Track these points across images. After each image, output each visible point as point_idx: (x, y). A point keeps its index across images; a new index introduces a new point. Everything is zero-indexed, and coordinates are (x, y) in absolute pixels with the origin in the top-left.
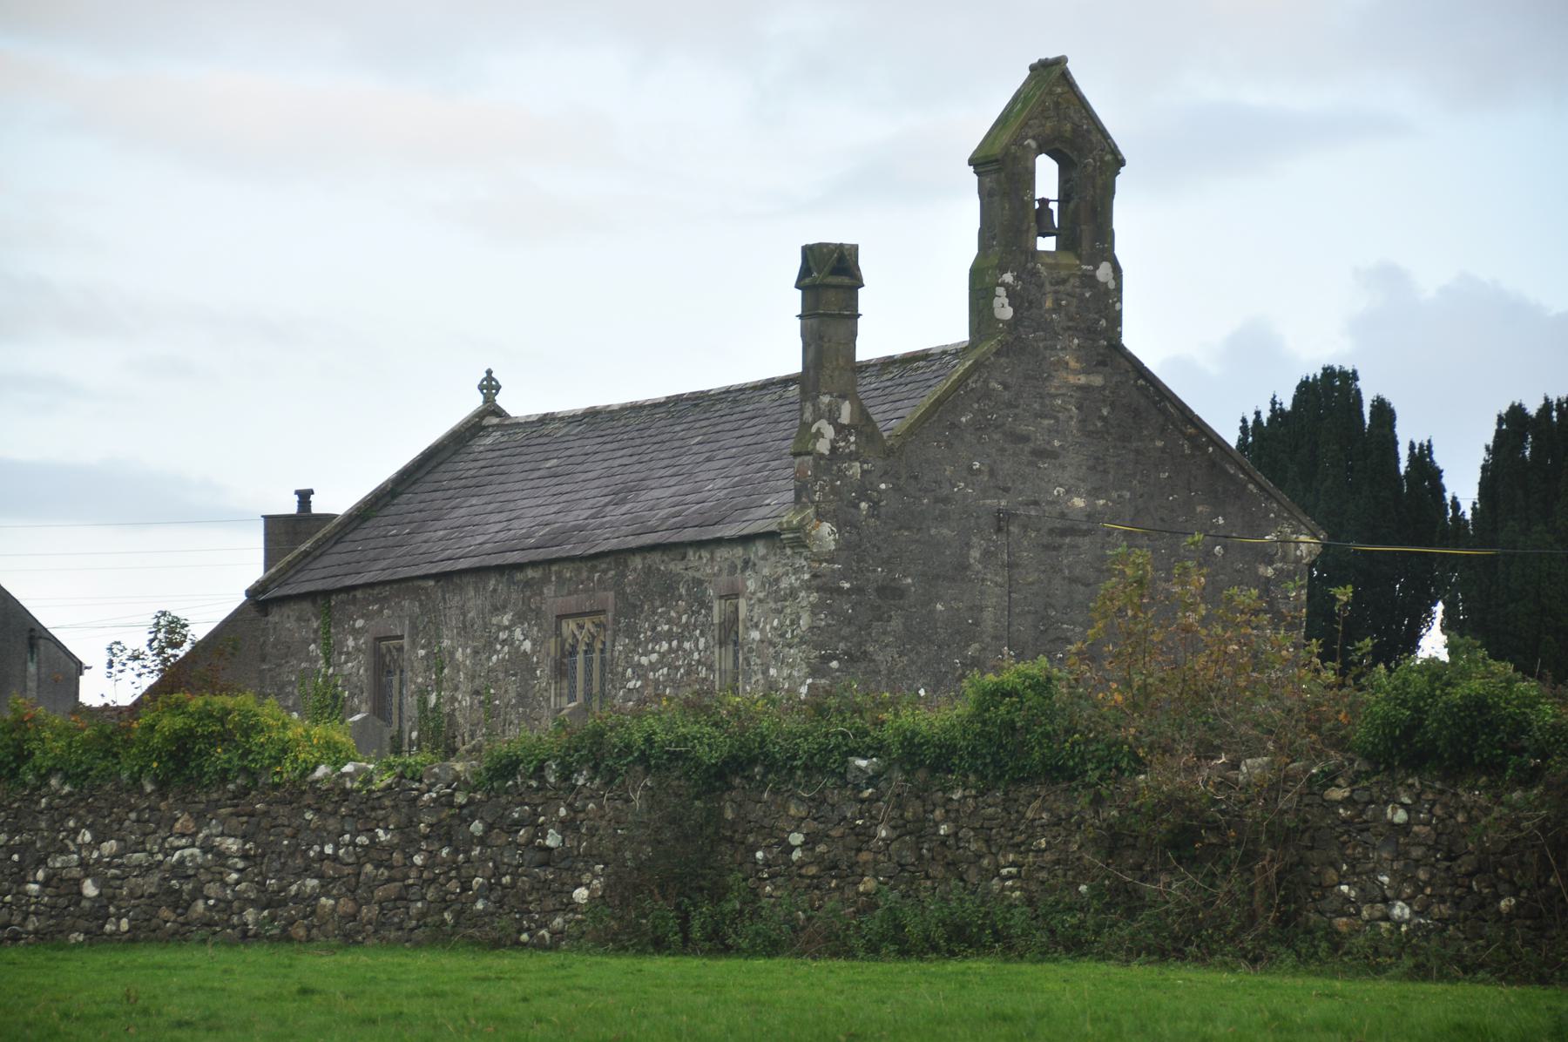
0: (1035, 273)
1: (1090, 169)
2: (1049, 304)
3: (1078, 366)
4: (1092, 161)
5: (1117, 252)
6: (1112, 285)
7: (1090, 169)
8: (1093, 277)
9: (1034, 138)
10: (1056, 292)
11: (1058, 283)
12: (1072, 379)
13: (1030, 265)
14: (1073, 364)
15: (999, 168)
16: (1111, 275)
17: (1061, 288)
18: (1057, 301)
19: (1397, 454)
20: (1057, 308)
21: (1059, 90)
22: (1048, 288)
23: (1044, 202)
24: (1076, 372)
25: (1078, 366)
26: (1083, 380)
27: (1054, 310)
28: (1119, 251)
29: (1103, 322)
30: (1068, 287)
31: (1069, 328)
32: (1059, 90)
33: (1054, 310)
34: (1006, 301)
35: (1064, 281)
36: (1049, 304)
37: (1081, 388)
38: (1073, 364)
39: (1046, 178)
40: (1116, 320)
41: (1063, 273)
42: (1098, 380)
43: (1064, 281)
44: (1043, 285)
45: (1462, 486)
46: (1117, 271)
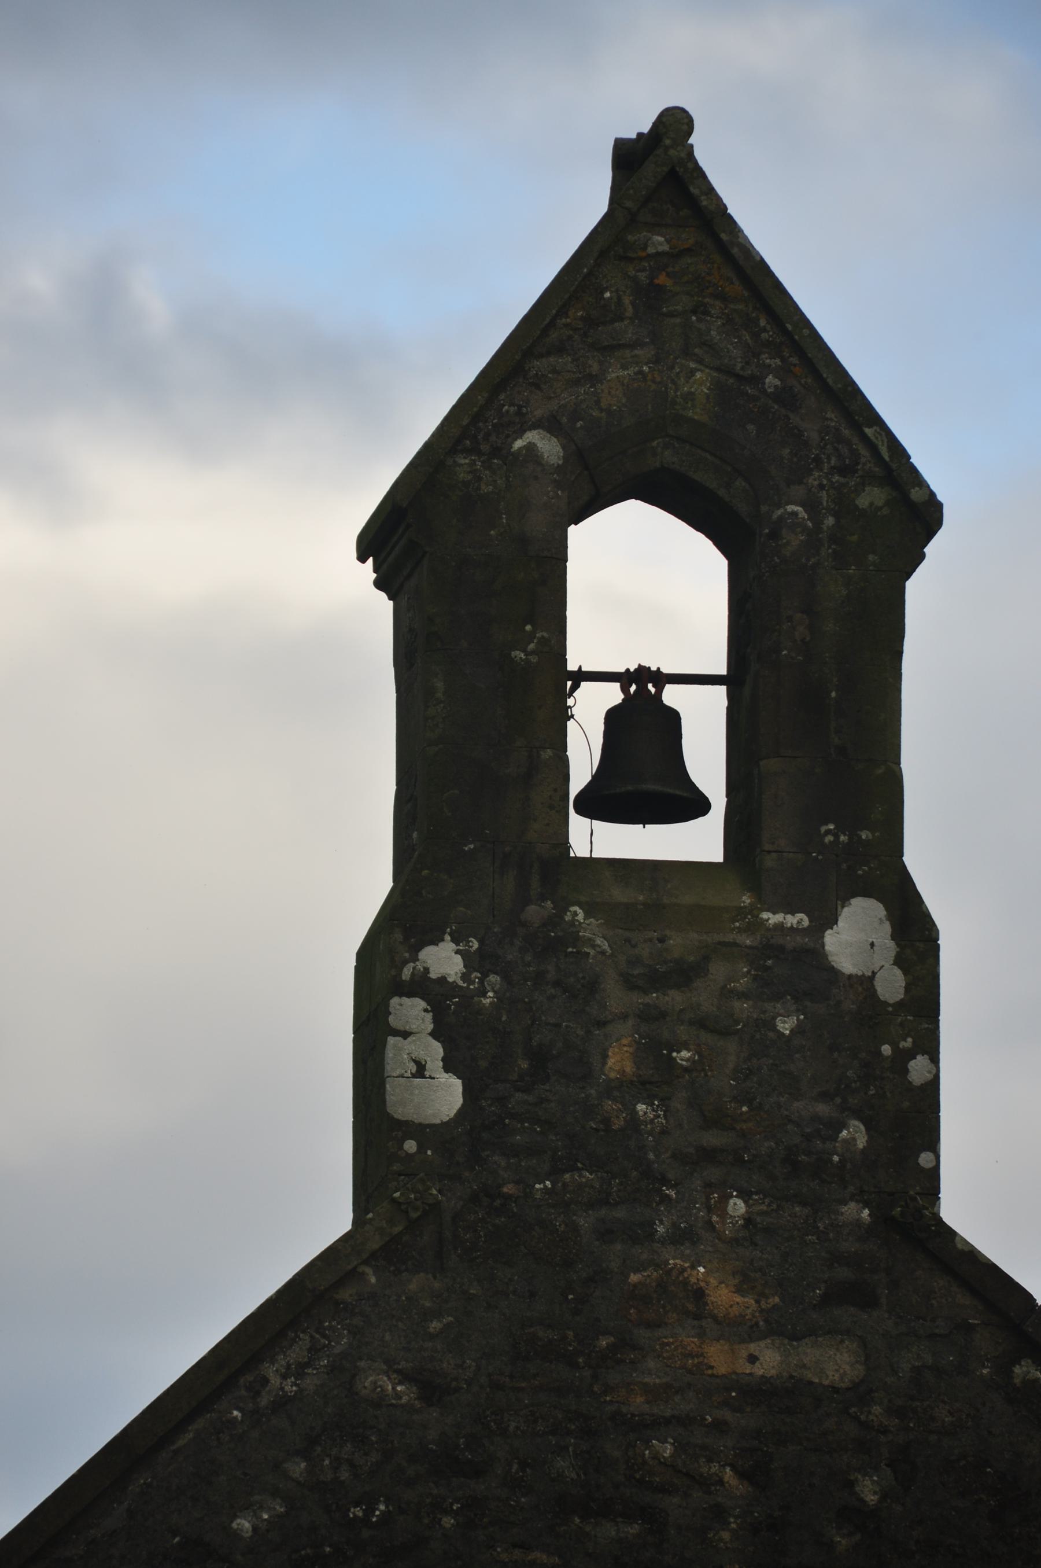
0: (557, 941)
1: (794, 541)
2: (619, 1060)
3: (743, 1304)
4: (830, 533)
5: (918, 858)
6: (891, 985)
7: (794, 541)
8: (813, 957)
9: (551, 425)
10: (650, 1016)
11: (656, 981)
12: (720, 1358)
13: (535, 913)
14: (723, 1297)
15: (462, 555)
16: (887, 947)
17: (674, 999)
18: (654, 1051)
19: (565, 763)
20: (656, 1076)
21: (659, 242)
22: (616, 997)
23: (643, 688)
24: (738, 1330)
25: (743, 1304)
26: (769, 1360)
27: (642, 1087)
28: (926, 856)
29: (855, 1134)
30: (703, 996)
31: (709, 1155)
32: (659, 242)
33: (642, 1087)
34: (434, 1052)
35: (684, 974)
36: (619, 1060)
37: (757, 1393)
38: (723, 1297)
39: (644, 592)
40: (915, 1120)
41: (680, 943)
42: (834, 1363)
43: (684, 974)
44: (593, 986)
45: (371, 559)
46: (915, 935)
